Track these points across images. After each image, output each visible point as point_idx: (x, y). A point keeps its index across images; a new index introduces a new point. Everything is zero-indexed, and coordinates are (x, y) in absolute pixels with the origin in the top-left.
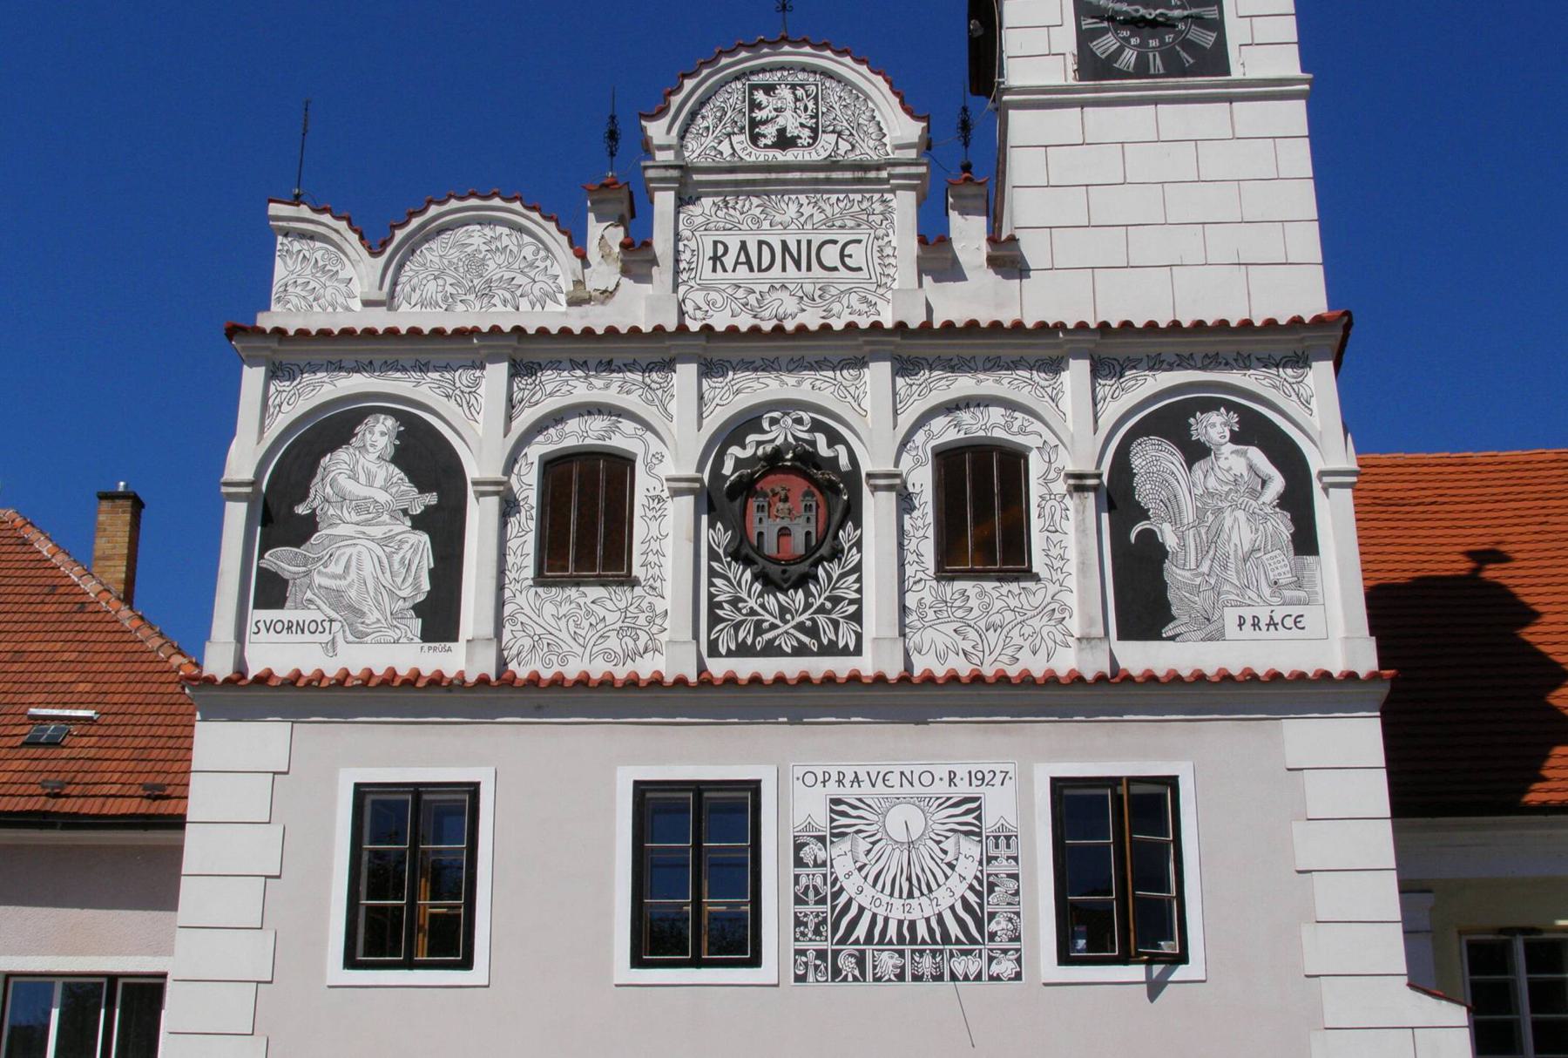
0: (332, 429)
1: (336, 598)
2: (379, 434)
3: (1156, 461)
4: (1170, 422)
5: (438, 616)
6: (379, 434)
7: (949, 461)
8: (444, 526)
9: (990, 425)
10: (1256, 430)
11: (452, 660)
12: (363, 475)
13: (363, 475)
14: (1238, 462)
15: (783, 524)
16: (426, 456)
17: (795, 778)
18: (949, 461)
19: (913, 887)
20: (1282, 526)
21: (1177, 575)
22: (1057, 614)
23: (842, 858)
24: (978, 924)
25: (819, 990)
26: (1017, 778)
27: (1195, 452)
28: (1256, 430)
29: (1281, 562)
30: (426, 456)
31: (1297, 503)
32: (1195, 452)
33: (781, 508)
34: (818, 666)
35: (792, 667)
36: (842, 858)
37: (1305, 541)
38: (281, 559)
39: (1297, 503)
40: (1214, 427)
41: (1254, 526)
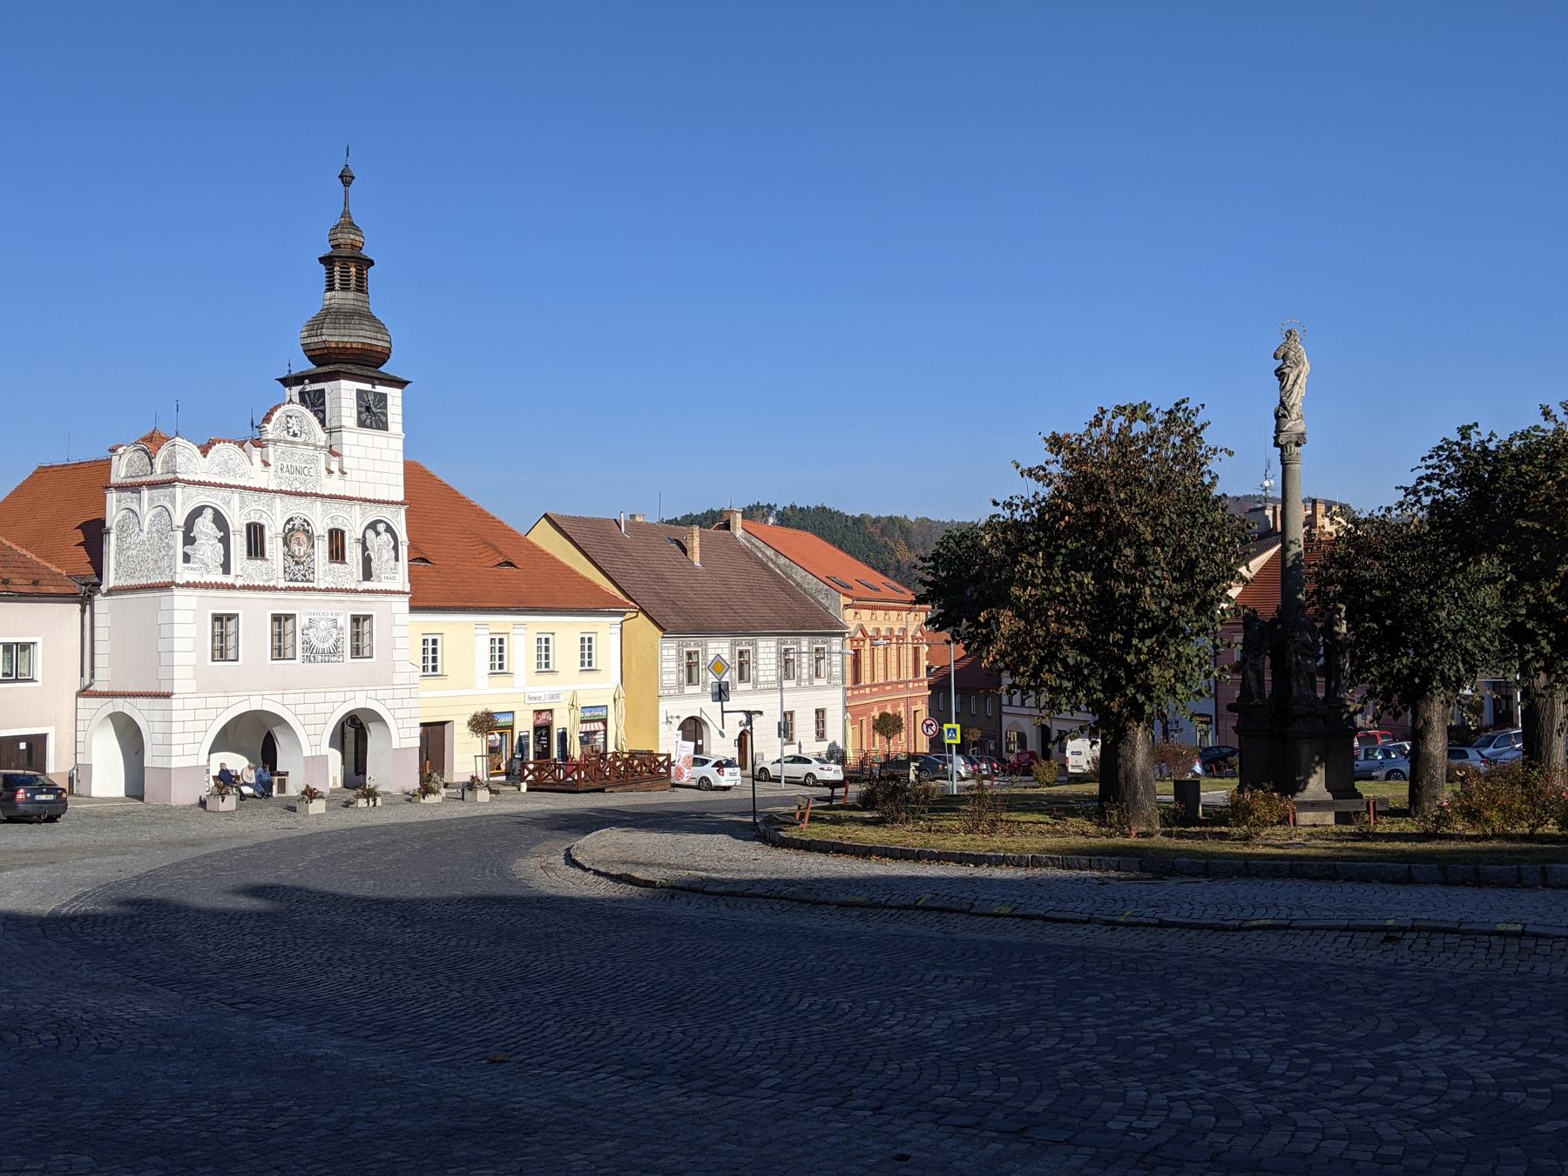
1: (202, 561)
2: (208, 514)
3: (370, 534)
4: (373, 526)
5: (226, 567)
6: (208, 514)
8: (225, 541)
11: (229, 580)
12: (205, 525)
13: (205, 525)
14: (386, 537)
16: (220, 521)
19: (324, 640)
20: (393, 554)
21: (373, 565)
22: (351, 574)
24: (335, 651)
27: (378, 534)
28: (389, 529)
31: (396, 548)
32: (378, 534)
34: (306, 585)
37: (397, 559)
38: (188, 549)
39: (396, 548)
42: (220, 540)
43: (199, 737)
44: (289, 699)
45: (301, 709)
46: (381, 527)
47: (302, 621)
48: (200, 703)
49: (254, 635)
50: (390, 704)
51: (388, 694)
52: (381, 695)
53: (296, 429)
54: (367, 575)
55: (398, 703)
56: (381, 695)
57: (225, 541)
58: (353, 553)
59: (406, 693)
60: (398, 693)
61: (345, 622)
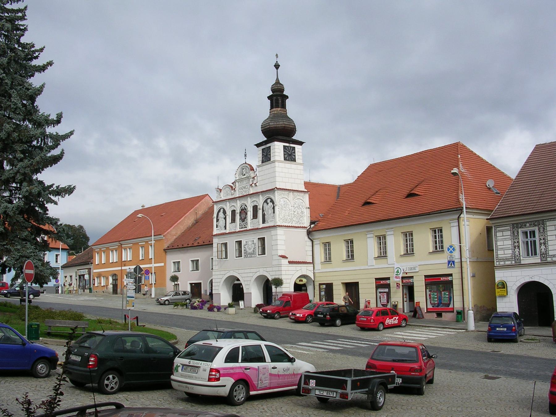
0: (219, 211)
2: (222, 210)
3: (265, 204)
4: (266, 201)
6: (222, 210)
8: (225, 218)
9: (255, 204)
14: (270, 204)
16: (225, 212)
19: (250, 249)
21: (266, 217)
23: (246, 246)
24: (254, 253)
29: (272, 214)
32: (268, 204)
36: (246, 246)
40: (269, 201)
41: (271, 211)
44: (240, 271)
46: (269, 201)
49: (232, 248)
52: (268, 269)
53: (244, 173)
54: (264, 222)
56: (268, 269)
60: (274, 269)
61: (256, 241)
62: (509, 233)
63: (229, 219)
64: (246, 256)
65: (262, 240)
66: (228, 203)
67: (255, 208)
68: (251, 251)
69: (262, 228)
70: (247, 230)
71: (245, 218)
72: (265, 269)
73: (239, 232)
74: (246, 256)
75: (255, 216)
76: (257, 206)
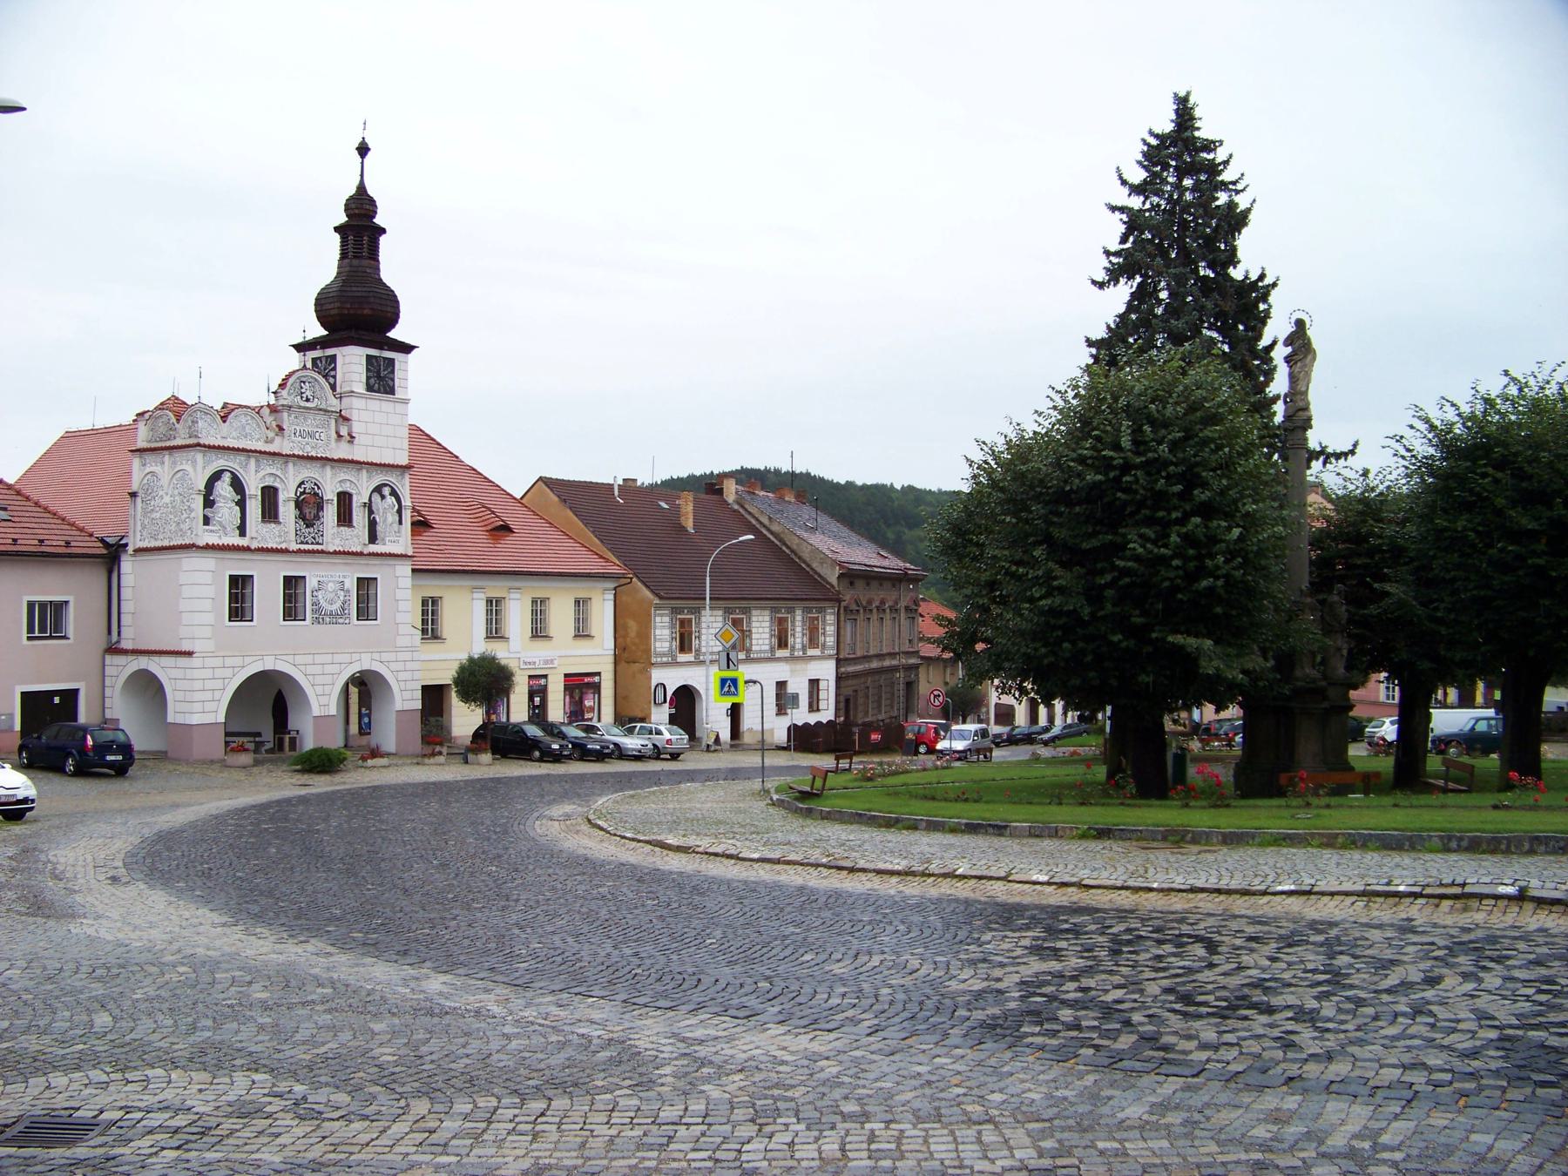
0: (216, 476)
1: (220, 523)
2: (227, 477)
3: (376, 497)
4: (378, 489)
5: (243, 533)
6: (227, 477)
7: (339, 495)
8: (242, 504)
9: (347, 487)
10: (394, 493)
11: (243, 542)
12: (224, 488)
13: (224, 488)
14: (391, 500)
15: (309, 511)
16: (237, 485)
17: (314, 574)
18: (339, 495)
19: (331, 602)
21: (379, 528)
23: (320, 595)
25: (316, 626)
26: (349, 576)
27: (383, 497)
28: (394, 493)
29: (396, 526)
30: (237, 485)
31: (399, 512)
32: (383, 497)
33: (310, 506)
34: (316, 547)
35: (310, 547)
36: (320, 595)
37: (400, 522)
38: (208, 512)
39: (399, 512)
40: (386, 491)
41: (392, 517)
42: (237, 504)
43: (217, 695)
44: (299, 660)
45: (310, 670)
46: (386, 491)
47: (311, 583)
48: (218, 662)
50: (394, 666)
51: (391, 656)
52: (385, 657)
53: (309, 393)
54: (373, 538)
55: (400, 666)
56: (385, 657)
57: (242, 504)
58: (359, 517)
59: (408, 656)
60: (401, 656)
62: (667, 619)
63: (254, 508)
64: (317, 621)
65: (365, 585)
66: (253, 461)
67: (345, 499)
68: (336, 607)
69: (335, 553)
70: (322, 552)
71: (317, 517)
72: (376, 656)
73: (299, 551)
74: (317, 621)
75: (345, 518)
76: (350, 495)
